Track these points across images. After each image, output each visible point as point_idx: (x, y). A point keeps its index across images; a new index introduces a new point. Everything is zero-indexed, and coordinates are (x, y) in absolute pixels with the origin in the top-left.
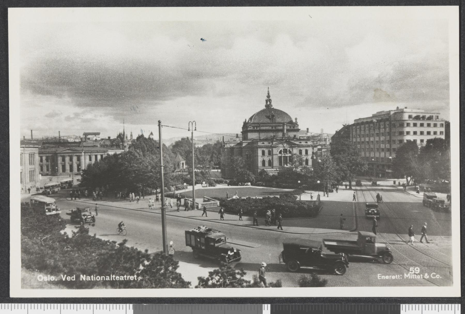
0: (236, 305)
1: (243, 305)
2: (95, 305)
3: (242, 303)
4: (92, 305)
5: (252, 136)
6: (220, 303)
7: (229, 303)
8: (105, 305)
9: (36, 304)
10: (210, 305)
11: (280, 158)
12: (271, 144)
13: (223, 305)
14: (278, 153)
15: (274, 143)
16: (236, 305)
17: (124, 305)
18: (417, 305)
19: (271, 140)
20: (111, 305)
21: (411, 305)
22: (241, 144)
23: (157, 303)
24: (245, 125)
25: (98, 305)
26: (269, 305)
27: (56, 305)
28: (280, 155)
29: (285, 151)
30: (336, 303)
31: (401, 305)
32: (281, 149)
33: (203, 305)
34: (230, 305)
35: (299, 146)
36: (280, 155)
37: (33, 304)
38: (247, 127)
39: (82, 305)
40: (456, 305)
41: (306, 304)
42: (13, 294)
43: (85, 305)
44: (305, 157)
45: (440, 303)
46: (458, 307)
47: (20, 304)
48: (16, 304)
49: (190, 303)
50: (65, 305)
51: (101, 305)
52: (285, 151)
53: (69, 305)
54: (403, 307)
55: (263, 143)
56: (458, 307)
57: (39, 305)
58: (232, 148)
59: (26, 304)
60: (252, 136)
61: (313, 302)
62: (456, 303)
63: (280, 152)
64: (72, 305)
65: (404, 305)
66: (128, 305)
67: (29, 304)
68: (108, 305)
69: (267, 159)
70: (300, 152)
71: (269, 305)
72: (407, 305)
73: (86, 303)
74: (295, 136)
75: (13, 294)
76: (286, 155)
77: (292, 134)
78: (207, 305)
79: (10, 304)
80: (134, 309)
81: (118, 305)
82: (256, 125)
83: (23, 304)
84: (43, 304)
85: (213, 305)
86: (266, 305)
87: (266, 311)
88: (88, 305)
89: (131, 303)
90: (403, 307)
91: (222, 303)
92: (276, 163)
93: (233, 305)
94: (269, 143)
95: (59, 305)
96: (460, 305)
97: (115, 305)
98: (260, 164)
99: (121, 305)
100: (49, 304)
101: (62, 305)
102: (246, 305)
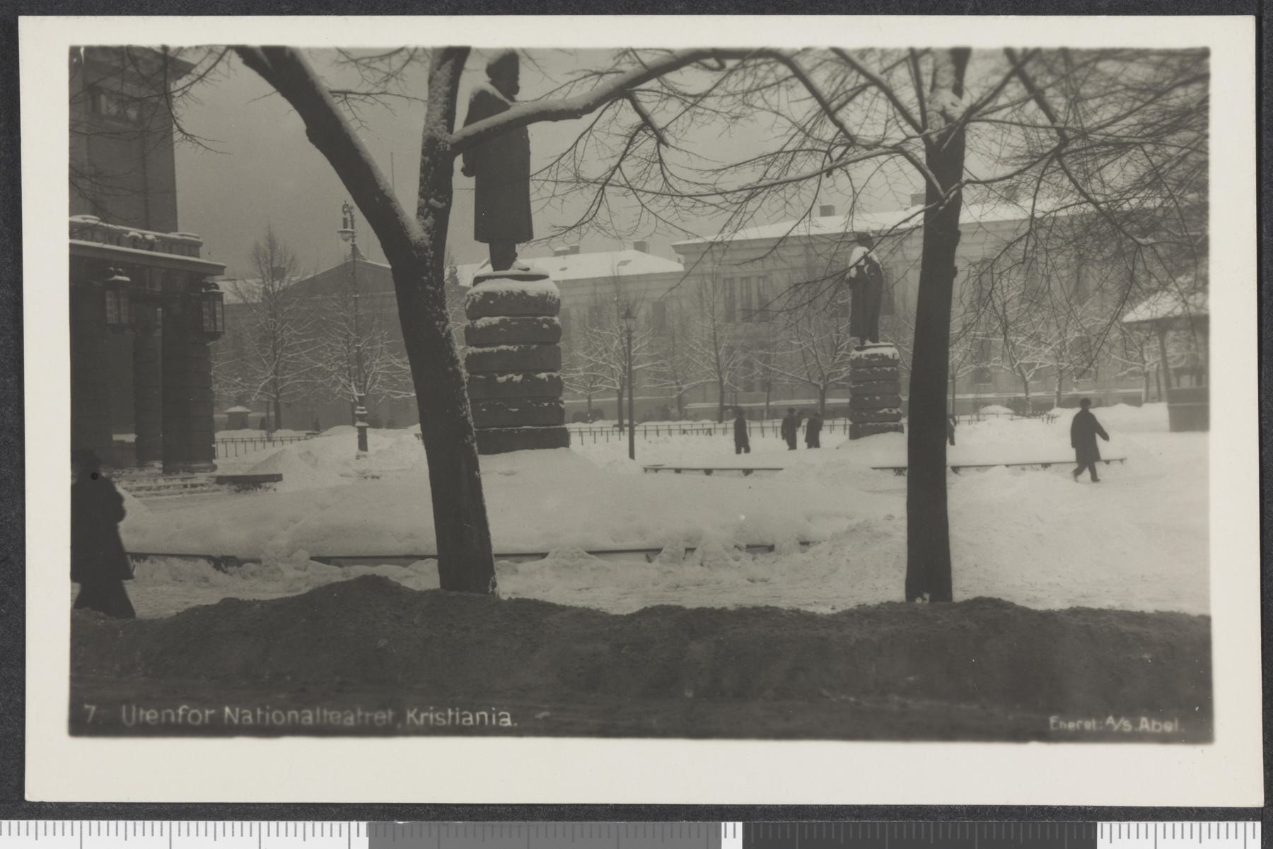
0: (649, 825)
1: (668, 824)
2: (264, 824)
3: (666, 819)
4: (255, 824)
6: (605, 819)
7: (629, 819)
8: (291, 824)
9: (103, 823)
10: (577, 824)
13: (613, 824)
16: (649, 824)
17: (345, 824)
18: (1142, 824)
20: (309, 824)
21: (1124, 825)
23: (434, 819)
25: (273, 824)
26: (739, 825)
27: (157, 823)
30: (922, 818)
31: (1099, 824)
33: (560, 824)
34: (632, 825)
37: (95, 823)
39: (229, 824)
40: (1250, 824)
41: (842, 821)
42: (35, 791)
43: (237, 824)
45: (1204, 820)
46: (1254, 830)
47: (59, 823)
48: (50, 823)
49: (524, 819)
50: (184, 823)
51: (282, 824)
53: (193, 823)
54: (1104, 828)
56: (1254, 830)
57: (112, 823)
59: (77, 823)
61: (858, 817)
62: (1248, 820)
64: (202, 823)
65: (1106, 825)
66: (354, 824)
67: (86, 823)
68: (300, 824)
71: (739, 825)
72: (1115, 825)
73: (241, 819)
75: (35, 791)
78: (569, 825)
79: (32, 823)
80: (371, 834)
81: (327, 824)
83: (68, 823)
84: (121, 823)
85: (587, 824)
86: (730, 825)
87: (732, 840)
88: (246, 824)
89: (363, 820)
90: (1104, 828)
91: (610, 819)
93: (640, 824)
95: (166, 823)
96: (1258, 824)
97: (318, 824)
99: (336, 824)
100: (139, 823)
101: (175, 823)
102: (676, 824)
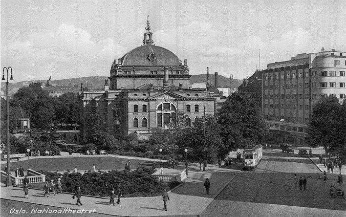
5: (122, 84)
11: (160, 115)
12: (147, 95)
14: (157, 109)
15: (151, 94)
19: (148, 89)
22: (105, 95)
24: (113, 71)
28: (160, 112)
29: (167, 106)
32: (161, 103)
35: (185, 99)
36: (160, 112)
38: (116, 71)
44: (195, 115)
52: (167, 106)
55: (136, 95)
58: (93, 101)
60: (122, 84)
63: (160, 108)
69: (140, 116)
70: (188, 107)
74: (181, 85)
76: (168, 112)
77: (177, 83)
82: (128, 68)
92: (154, 124)
94: (145, 95)
98: (131, 124)
